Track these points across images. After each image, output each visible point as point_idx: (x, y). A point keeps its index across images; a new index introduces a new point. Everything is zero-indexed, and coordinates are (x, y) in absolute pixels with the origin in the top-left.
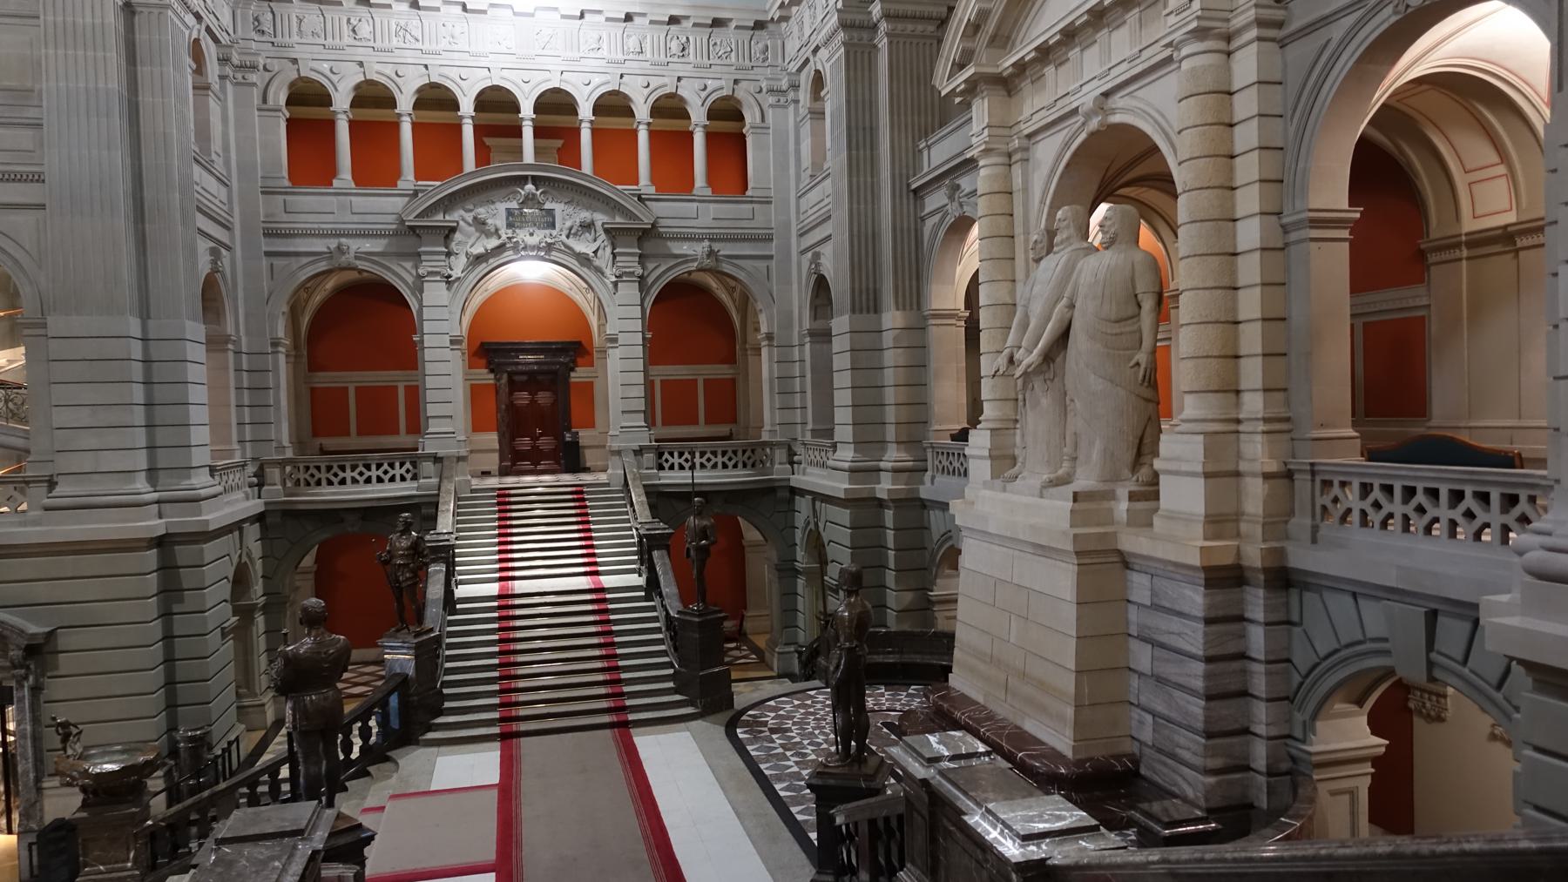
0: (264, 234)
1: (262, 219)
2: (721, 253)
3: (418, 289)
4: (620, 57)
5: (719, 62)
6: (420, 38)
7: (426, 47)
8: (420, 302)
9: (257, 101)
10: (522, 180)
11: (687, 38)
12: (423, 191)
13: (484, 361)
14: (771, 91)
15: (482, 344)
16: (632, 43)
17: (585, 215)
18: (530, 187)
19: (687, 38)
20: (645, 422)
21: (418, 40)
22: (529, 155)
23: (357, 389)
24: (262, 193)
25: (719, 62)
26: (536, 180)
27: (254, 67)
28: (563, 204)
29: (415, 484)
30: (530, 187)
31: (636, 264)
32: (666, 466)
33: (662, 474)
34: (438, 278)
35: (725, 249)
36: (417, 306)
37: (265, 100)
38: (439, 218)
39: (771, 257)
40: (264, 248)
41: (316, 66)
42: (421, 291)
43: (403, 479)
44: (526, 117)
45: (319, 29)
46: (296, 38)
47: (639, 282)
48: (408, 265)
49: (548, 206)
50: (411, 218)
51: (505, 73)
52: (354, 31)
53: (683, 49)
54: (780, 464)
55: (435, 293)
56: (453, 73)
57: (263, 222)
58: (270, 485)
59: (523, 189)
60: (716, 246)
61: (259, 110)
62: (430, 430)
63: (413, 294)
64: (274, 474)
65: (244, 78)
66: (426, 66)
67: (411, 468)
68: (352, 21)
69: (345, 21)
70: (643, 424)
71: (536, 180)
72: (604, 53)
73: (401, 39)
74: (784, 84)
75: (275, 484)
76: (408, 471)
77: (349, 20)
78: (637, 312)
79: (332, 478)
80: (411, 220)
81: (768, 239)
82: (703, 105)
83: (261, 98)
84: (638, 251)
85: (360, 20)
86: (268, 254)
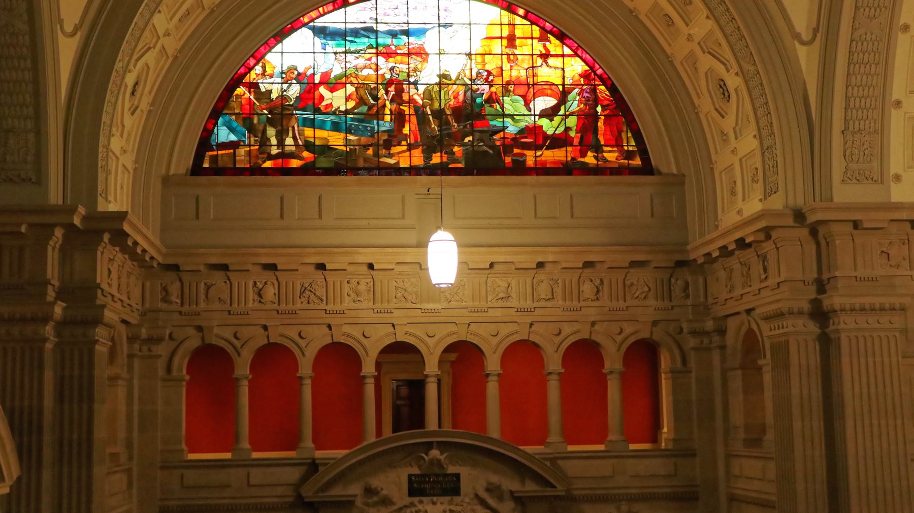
4: (529, 304)
5: (636, 302)
6: (324, 298)
7: (330, 307)
9: (161, 372)
11: (601, 280)
14: (694, 333)
16: (543, 290)
17: (495, 479)
18: (435, 453)
19: (601, 280)
21: (322, 300)
22: (432, 422)
25: (636, 302)
26: (443, 446)
27: (160, 340)
30: (435, 453)
37: (169, 370)
41: (220, 335)
45: (226, 296)
46: (202, 305)
51: (409, 329)
52: (260, 295)
53: (598, 292)
56: (356, 332)
59: (427, 455)
61: (164, 380)
65: (150, 350)
66: (329, 327)
68: (258, 284)
69: (251, 284)
71: (443, 446)
72: (514, 303)
73: (304, 300)
74: (709, 325)
77: (255, 283)
82: (618, 350)
85: (266, 283)
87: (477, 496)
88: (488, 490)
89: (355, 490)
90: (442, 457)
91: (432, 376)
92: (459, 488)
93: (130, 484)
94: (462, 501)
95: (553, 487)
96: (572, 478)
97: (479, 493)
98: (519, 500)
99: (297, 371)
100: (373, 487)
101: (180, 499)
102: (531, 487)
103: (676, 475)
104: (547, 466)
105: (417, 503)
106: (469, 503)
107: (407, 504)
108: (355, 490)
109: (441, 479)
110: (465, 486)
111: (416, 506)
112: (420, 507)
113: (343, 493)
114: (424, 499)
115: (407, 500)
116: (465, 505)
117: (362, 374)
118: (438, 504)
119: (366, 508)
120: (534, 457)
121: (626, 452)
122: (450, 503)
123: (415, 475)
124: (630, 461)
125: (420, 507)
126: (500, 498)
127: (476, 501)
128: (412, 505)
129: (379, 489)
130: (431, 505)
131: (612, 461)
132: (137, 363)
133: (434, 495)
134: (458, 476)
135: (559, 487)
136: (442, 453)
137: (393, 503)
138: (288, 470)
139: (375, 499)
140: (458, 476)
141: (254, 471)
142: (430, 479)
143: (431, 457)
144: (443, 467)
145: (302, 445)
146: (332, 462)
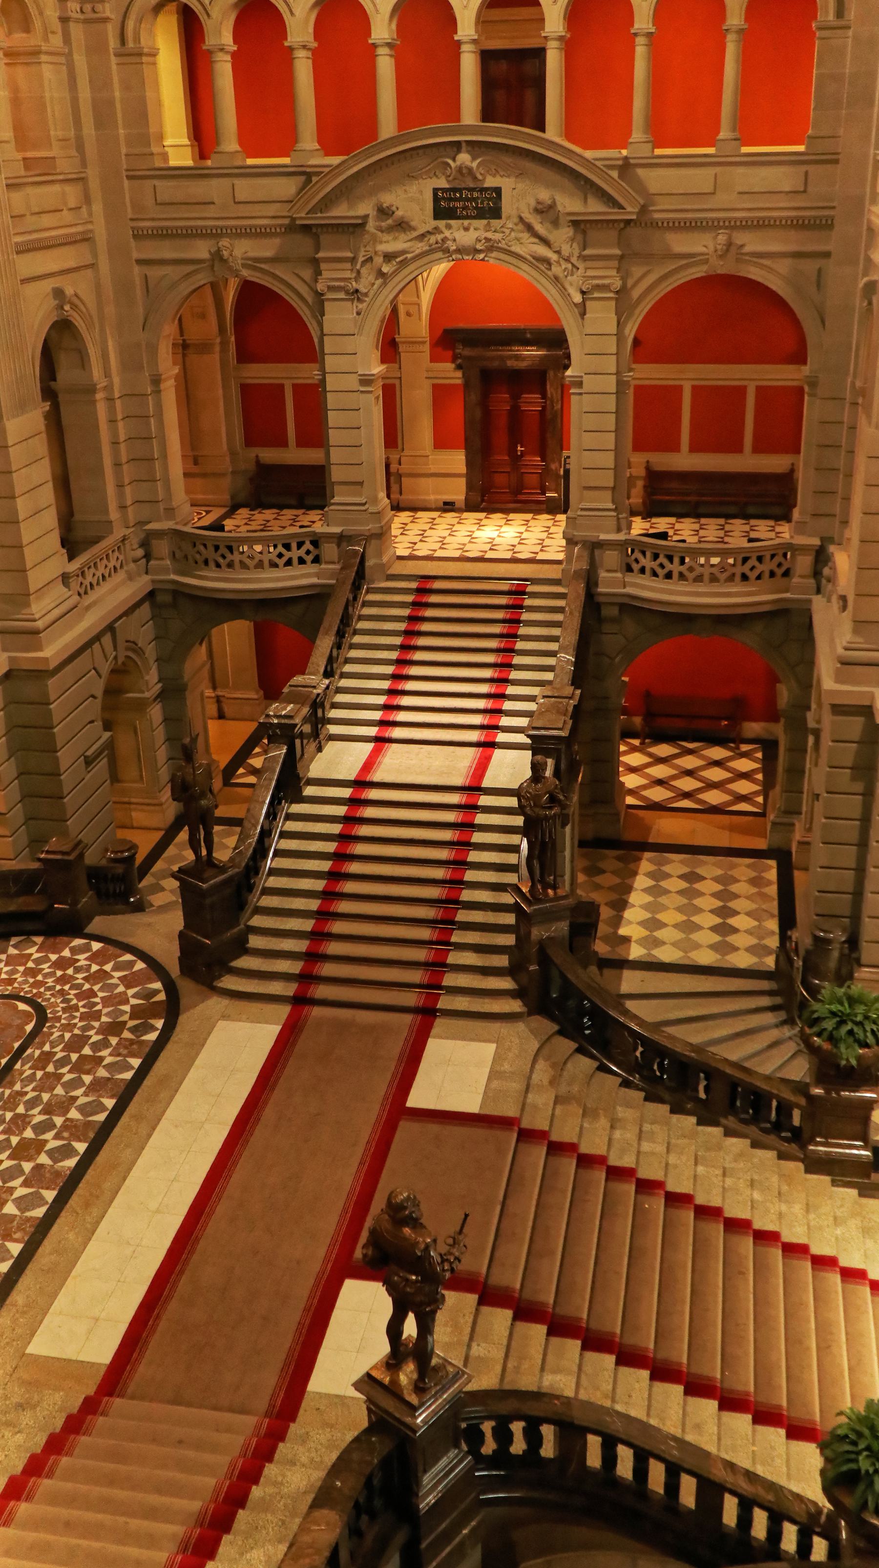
0: (134, 236)
1: (130, 216)
2: (747, 249)
3: (319, 310)
8: (321, 325)
9: (113, 43)
10: (457, 146)
12: (317, 174)
13: (449, 353)
18: (464, 158)
20: (613, 502)
23: (295, 387)
24: (128, 177)
28: (512, 179)
30: (464, 158)
31: (614, 273)
32: (635, 567)
33: (630, 578)
34: (342, 295)
35: (752, 242)
36: (319, 333)
37: (123, 41)
38: (341, 211)
39: (827, 255)
40: (135, 255)
42: (323, 314)
43: (301, 561)
44: (465, 39)
47: (617, 299)
48: (307, 274)
49: (490, 182)
54: (801, 576)
57: (132, 219)
58: (157, 559)
59: (454, 160)
60: (740, 238)
61: (116, 55)
62: (336, 499)
63: (315, 317)
64: (162, 547)
65: (94, 11)
67: (311, 548)
70: (611, 506)
75: (162, 559)
76: (308, 552)
78: (611, 345)
79: (221, 560)
80: (302, 216)
81: (824, 225)
83: (118, 42)
86: (139, 262)
87: (521, 219)
89: (365, 208)
90: (474, 165)
91: (466, 43)
92: (501, 208)
93: (87, 199)
94: (502, 227)
95: (621, 207)
96: (654, 195)
97: (522, 215)
98: (578, 225)
99: (369, 35)
100: (385, 205)
101: (153, 219)
102: (595, 207)
103: (805, 191)
104: (613, 178)
105: (443, 229)
106: (512, 230)
107: (430, 229)
108: (365, 208)
109: (475, 195)
110: (507, 205)
111: (442, 232)
112: (447, 233)
113: (351, 213)
115: (433, 223)
116: (507, 231)
117: (370, 41)
118: (472, 229)
119: (379, 233)
120: (594, 165)
121: (737, 156)
122: (487, 228)
123: (444, 190)
124: (741, 170)
125: (447, 233)
126: (555, 223)
127: (521, 227)
128: (437, 230)
129: (394, 208)
130: (462, 231)
131: (711, 171)
132: (77, 31)
133: (467, 217)
134: (498, 191)
135: (629, 209)
136: (474, 159)
137: (414, 229)
138: (283, 180)
139: (390, 222)
140: (498, 191)
141: (239, 183)
142: (461, 195)
143: (458, 163)
144: (475, 178)
145: (299, 146)
146: (327, 170)
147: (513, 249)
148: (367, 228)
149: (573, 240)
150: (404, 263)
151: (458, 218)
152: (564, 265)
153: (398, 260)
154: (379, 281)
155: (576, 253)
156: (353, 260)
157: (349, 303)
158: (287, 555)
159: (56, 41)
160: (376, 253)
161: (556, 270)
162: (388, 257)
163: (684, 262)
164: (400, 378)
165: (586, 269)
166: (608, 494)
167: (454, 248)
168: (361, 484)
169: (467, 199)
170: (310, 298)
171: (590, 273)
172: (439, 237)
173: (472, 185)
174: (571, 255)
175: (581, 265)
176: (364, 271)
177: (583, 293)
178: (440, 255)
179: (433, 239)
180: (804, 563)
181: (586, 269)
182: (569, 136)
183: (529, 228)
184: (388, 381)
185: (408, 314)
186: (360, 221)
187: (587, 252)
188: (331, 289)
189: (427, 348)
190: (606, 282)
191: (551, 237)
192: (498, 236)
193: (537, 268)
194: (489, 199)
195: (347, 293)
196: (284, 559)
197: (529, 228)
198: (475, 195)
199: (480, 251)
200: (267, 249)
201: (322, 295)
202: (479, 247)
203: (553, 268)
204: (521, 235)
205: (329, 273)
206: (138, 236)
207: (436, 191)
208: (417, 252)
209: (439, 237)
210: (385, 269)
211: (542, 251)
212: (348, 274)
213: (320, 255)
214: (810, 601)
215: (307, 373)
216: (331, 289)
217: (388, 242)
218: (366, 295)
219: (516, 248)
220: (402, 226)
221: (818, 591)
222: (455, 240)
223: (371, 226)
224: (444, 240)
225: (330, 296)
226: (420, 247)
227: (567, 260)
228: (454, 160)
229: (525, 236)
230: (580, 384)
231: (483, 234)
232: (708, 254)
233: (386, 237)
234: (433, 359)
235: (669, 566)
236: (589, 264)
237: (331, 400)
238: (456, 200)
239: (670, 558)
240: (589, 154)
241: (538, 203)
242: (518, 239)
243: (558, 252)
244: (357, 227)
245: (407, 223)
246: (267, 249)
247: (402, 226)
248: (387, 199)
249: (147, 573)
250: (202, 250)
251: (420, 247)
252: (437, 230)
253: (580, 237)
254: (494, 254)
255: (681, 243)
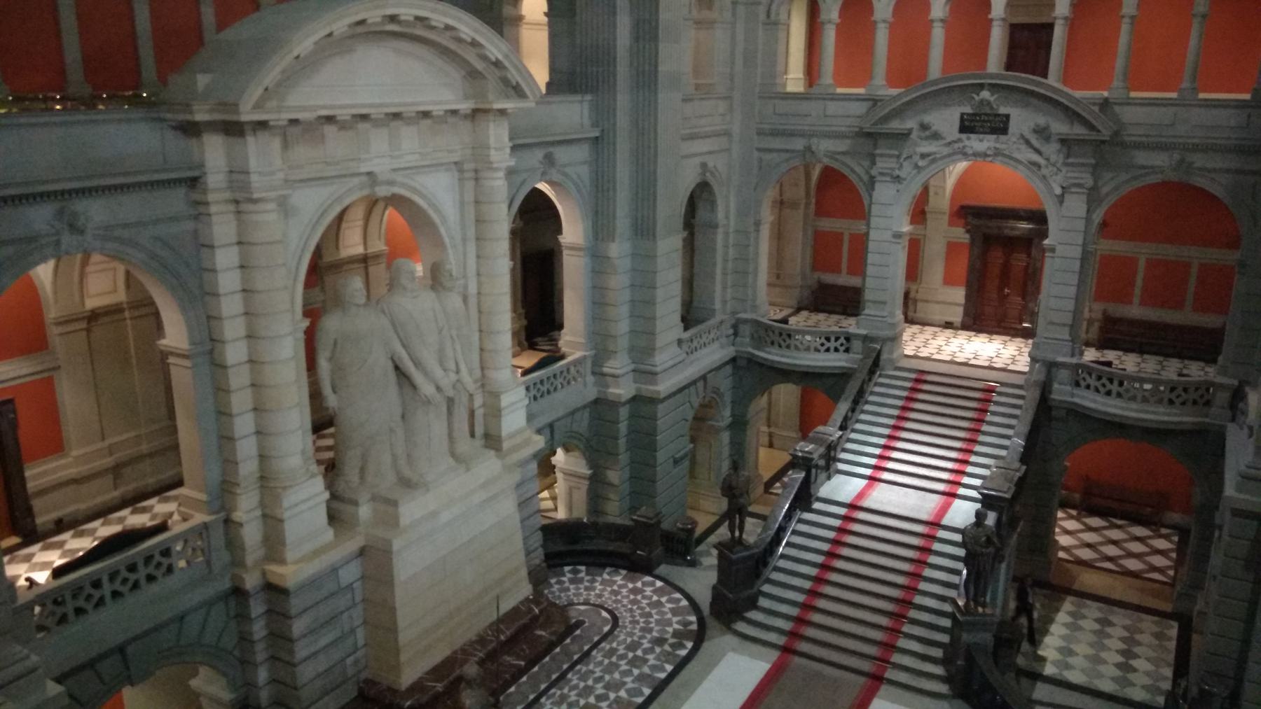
8: (871, 196)
9: (762, 17)
12: (881, 100)
13: (963, 221)
15: (963, 207)
17: (1042, 120)
18: (985, 94)
20: (1070, 335)
26: (994, 88)
29: (845, 356)
30: (985, 94)
31: (1088, 176)
32: (1083, 384)
33: (1076, 391)
34: (888, 179)
35: (1199, 160)
37: (768, 16)
38: (895, 125)
42: (873, 189)
43: (836, 350)
48: (866, 163)
50: (868, 126)
55: (884, 192)
59: (978, 95)
62: (866, 311)
64: (746, 330)
67: (844, 342)
71: (994, 88)
76: (842, 345)
78: (1081, 225)
79: (782, 343)
80: (867, 127)
84: (1093, 161)
86: (759, 150)
87: (1022, 136)
88: (1035, 131)
89: (910, 123)
90: (992, 99)
93: (731, 109)
106: (1015, 142)
109: (991, 118)
110: (1013, 127)
113: (899, 127)
114: (972, 136)
115: (958, 136)
122: (997, 141)
123: (968, 114)
127: (1022, 141)
128: (960, 140)
133: (982, 133)
134: (1008, 116)
136: (992, 95)
137: (943, 138)
139: (927, 133)
140: (1008, 116)
144: (992, 108)
146: (888, 98)
147: (1014, 155)
148: (912, 136)
149: (1059, 151)
150: (934, 161)
151: (976, 133)
152: (1051, 168)
153: (930, 158)
154: (915, 171)
155: (1061, 161)
156: (898, 157)
157: (891, 185)
158: (827, 345)
159: (728, 15)
160: (915, 153)
161: (1044, 171)
162: (923, 156)
163: (1143, 171)
164: (925, 235)
165: (1067, 172)
166: (1067, 330)
167: (971, 152)
168: (884, 303)
169: (984, 121)
170: (866, 178)
171: (1069, 175)
172: (961, 145)
173: (989, 112)
174: (1056, 162)
175: (1064, 169)
176: (905, 164)
177: (1063, 188)
178: (960, 156)
179: (956, 146)
180: (1222, 398)
181: (1067, 172)
182: (1065, 83)
183: (1028, 142)
184: (914, 237)
185: (936, 194)
186: (906, 132)
187: (1071, 160)
188: (882, 174)
189: (946, 218)
190: (1082, 181)
191: (1043, 149)
192: (1003, 146)
193: (1029, 169)
194: (1001, 122)
195: (892, 177)
196: (825, 347)
197: (1028, 142)
198: (991, 118)
199: (989, 156)
200: (842, 146)
201: (874, 177)
202: (989, 153)
203: (1042, 169)
204: (1020, 146)
205: (882, 164)
206: (760, 133)
207: (962, 115)
208: (945, 153)
209: (961, 145)
210: (921, 163)
211: (1035, 157)
212: (893, 165)
213: (878, 151)
214: (1223, 427)
215: (860, 227)
216: (882, 174)
217: (924, 146)
218: (905, 179)
219: (1017, 155)
220: (936, 136)
221: (1233, 420)
222: (972, 147)
223: (914, 135)
224: (964, 147)
225: (879, 178)
226: (946, 151)
227: (1054, 165)
228: (978, 95)
229: (1023, 147)
230: (1053, 250)
231: (992, 144)
232: (1164, 167)
233: (925, 143)
234: (951, 224)
235: (1109, 386)
236: (1070, 168)
237: (872, 246)
238: (977, 121)
239: (1111, 381)
240: (1078, 94)
241: (1038, 126)
242: (1018, 149)
243: (1048, 159)
244: (904, 136)
245: (940, 135)
246: (842, 146)
247: (936, 136)
248: (927, 119)
249: (733, 345)
250: (799, 144)
251: (946, 151)
252: (960, 140)
253: (1065, 150)
254: (1000, 158)
255: (1141, 158)
